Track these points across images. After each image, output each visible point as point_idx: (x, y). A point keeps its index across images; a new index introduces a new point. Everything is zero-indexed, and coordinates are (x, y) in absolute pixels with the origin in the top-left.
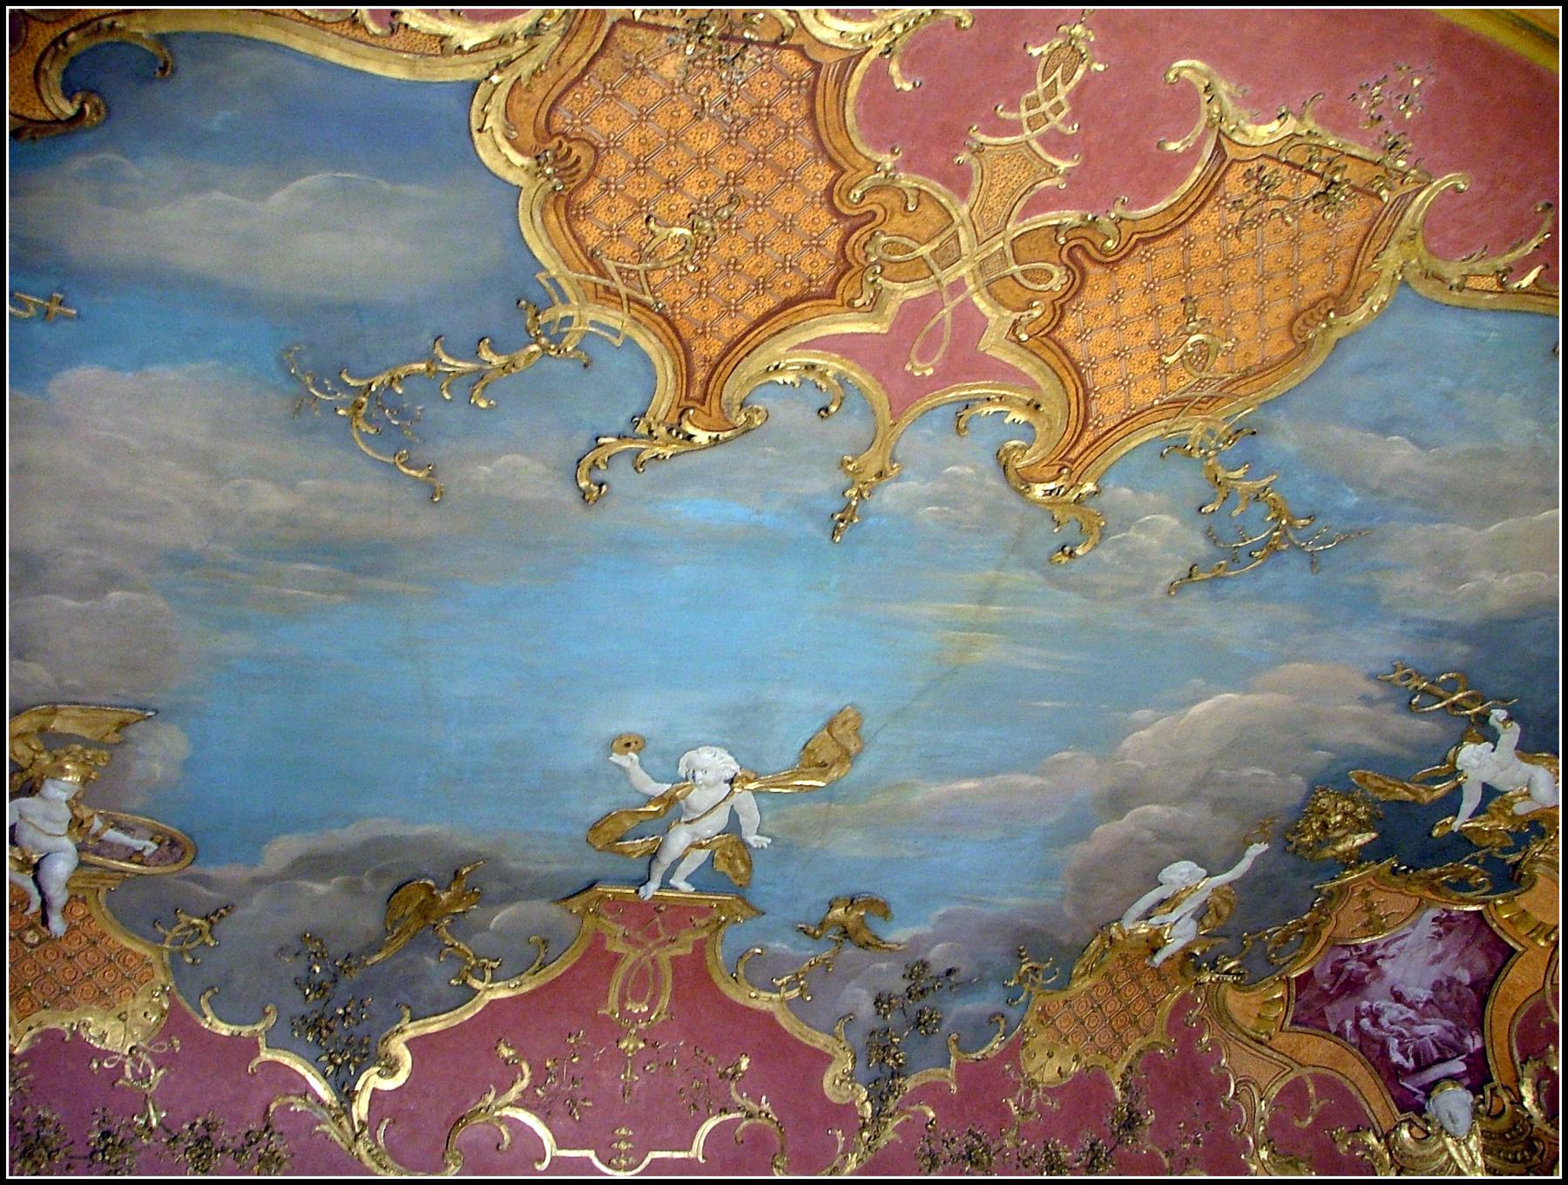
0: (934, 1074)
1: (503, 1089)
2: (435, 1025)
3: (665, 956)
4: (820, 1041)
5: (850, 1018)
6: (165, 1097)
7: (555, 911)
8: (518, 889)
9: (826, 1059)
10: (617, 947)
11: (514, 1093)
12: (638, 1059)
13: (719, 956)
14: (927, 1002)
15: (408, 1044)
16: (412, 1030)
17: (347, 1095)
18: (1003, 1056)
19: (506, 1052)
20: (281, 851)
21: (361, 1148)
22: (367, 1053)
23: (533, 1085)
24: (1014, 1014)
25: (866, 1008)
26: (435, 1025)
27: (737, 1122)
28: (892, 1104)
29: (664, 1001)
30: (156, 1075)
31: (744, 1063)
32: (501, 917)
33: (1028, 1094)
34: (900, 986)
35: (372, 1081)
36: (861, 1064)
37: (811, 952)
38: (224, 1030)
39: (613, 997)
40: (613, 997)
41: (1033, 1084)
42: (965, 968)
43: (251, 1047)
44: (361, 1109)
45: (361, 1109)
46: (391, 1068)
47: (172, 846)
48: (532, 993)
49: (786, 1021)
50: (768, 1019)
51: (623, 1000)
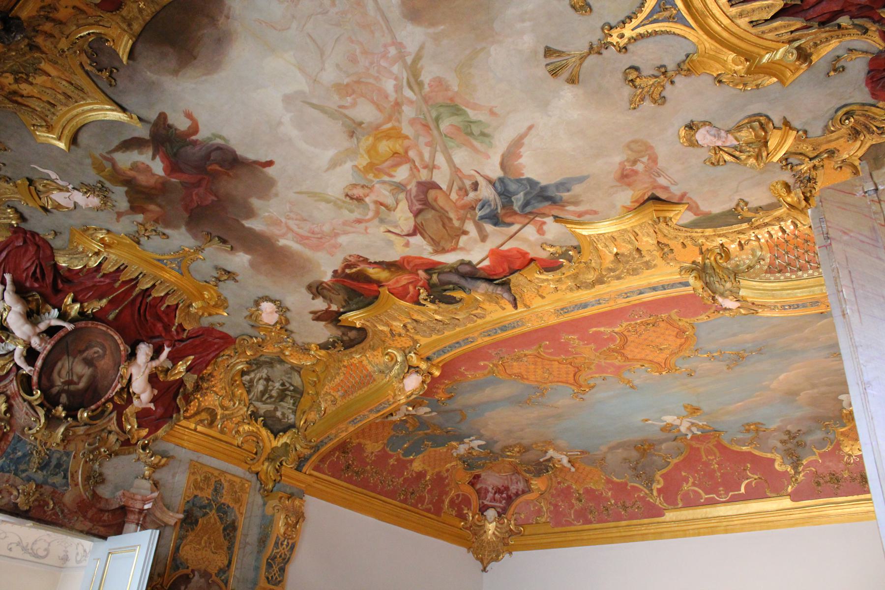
0: (813, 458)
1: (687, 483)
2: (664, 471)
3: (710, 445)
4: (769, 455)
5: (775, 448)
6: (613, 496)
7: (674, 443)
8: (661, 442)
9: (773, 461)
10: (698, 446)
11: (690, 484)
12: (720, 469)
13: (725, 442)
14: (796, 440)
15: (662, 476)
16: (660, 473)
17: (652, 490)
18: (833, 450)
19: (683, 474)
20: (604, 448)
21: (658, 503)
22: (650, 481)
23: (695, 480)
24: (832, 437)
25: (779, 445)
26: (664, 471)
27: (751, 482)
28: (801, 469)
29: (718, 454)
30: (610, 494)
31: (749, 465)
32: (663, 446)
33: (849, 458)
34: (786, 437)
35: (656, 486)
36: (785, 460)
37: (749, 436)
38: (618, 480)
39: (704, 457)
40: (704, 457)
41: (850, 456)
42: (804, 429)
43: (626, 484)
44: (655, 493)
45: (655, 493)
46: (658, 482)
47: (582, 452)
48: (683, 460)
49: (756, 453)
50: (750, 453)
51: (707, 457)
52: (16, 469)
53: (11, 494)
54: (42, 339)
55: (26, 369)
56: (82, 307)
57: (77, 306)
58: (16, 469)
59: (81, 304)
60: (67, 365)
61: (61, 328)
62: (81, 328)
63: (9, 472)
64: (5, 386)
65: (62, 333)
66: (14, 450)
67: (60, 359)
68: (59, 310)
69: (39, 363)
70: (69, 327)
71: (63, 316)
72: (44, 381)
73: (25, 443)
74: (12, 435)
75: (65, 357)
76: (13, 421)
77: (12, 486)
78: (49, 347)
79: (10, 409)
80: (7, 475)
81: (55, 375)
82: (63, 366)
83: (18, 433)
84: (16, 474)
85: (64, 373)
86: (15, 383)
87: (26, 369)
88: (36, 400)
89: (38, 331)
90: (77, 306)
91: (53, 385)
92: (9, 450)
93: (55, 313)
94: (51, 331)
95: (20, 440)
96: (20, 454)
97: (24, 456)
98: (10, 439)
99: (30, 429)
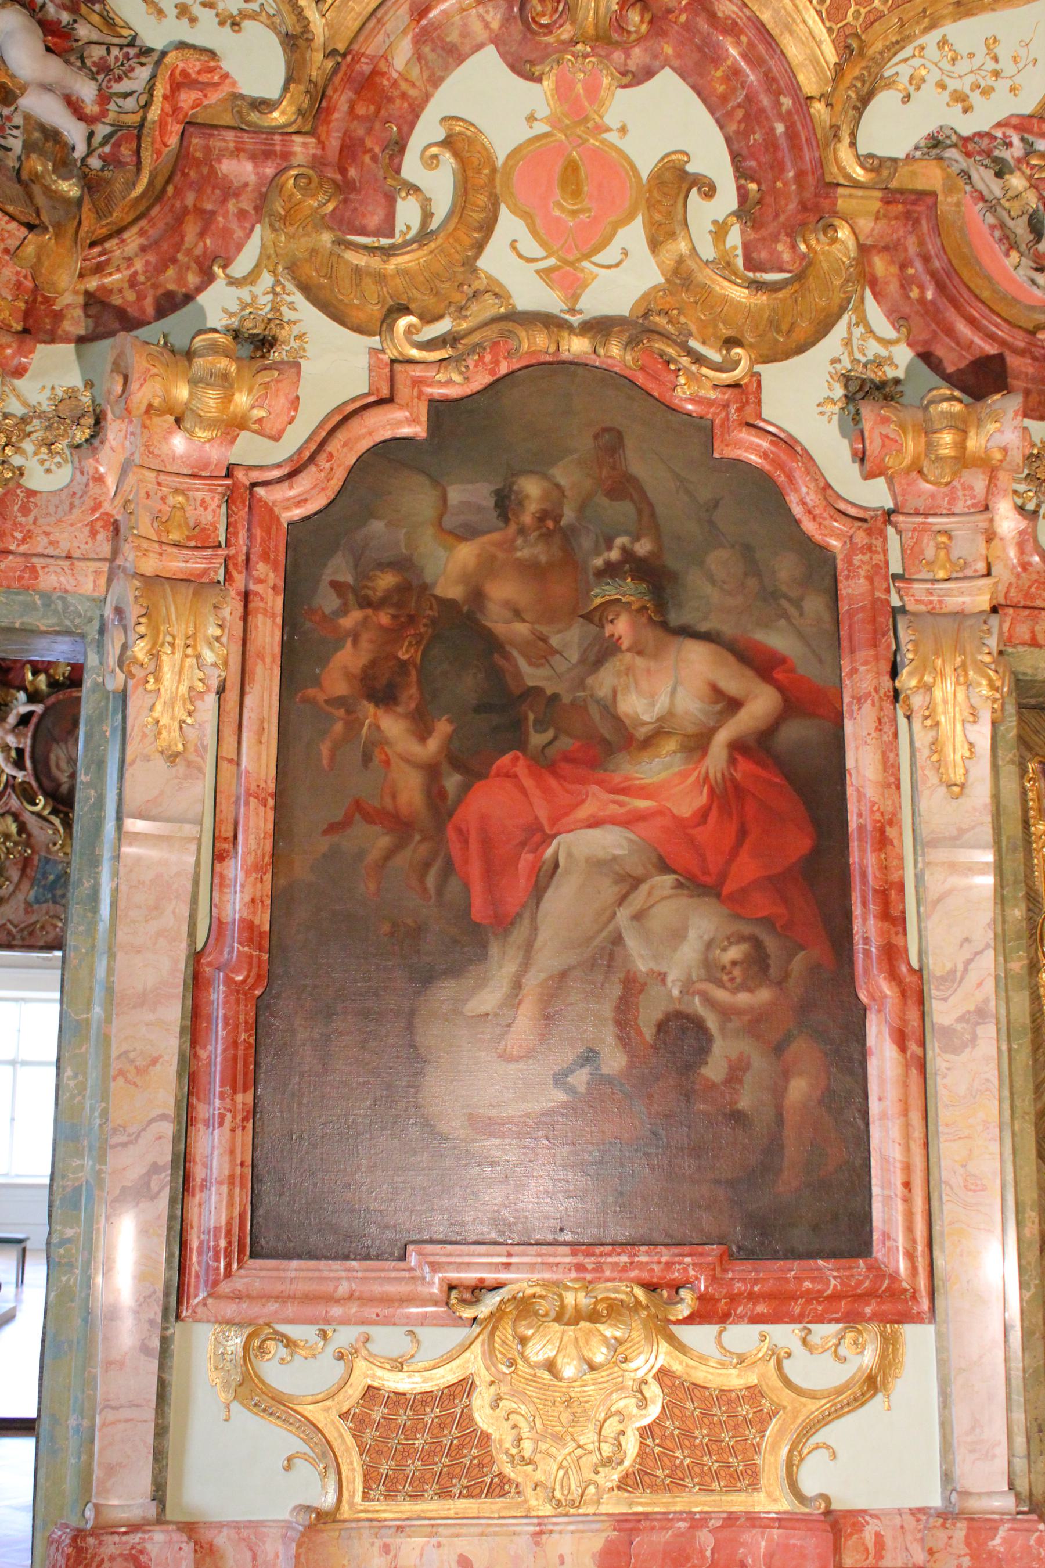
52: (54, 896)
53: (56, 926)
54: (17, 736)
55: (20, 776)
56: (48, 676)
57: (42, 678)
58: (54, 896)
59: (46, 672)
60: (62, 756)
61: (31, 714)
62: (54, 704)
63: (46, 901)
64: (6, 804)
65: (34, 720)
66: (45, 875)
67: (49, 752)
68: (25, 690)
69: (28, 763)
70: (38, 708)
71: (33, 697)
72: (46, 783)
73: (56, 863)
74: (36, 858)
75: (55, 745)
76: (33, 841)
77: (52, 917)
78: (29, 741)
79: (22, 828)
80: (45, 906)
81: (54, 771)
82: (58, 758)
83: (43, 854)
84: (55, 902)
85: (63, 765)
86: (14, 796)
87: (20, 776)
88: (44, 808)
89: (8, 727)
90: (42, 678)
91: (59, 785)
92: (39, 876)
93: (22, 696)
94: (24, 720)
95: (47, 861)
96: (52, 877)
97: (58, 877)
98: (36, 862)
99: (55, 844)
